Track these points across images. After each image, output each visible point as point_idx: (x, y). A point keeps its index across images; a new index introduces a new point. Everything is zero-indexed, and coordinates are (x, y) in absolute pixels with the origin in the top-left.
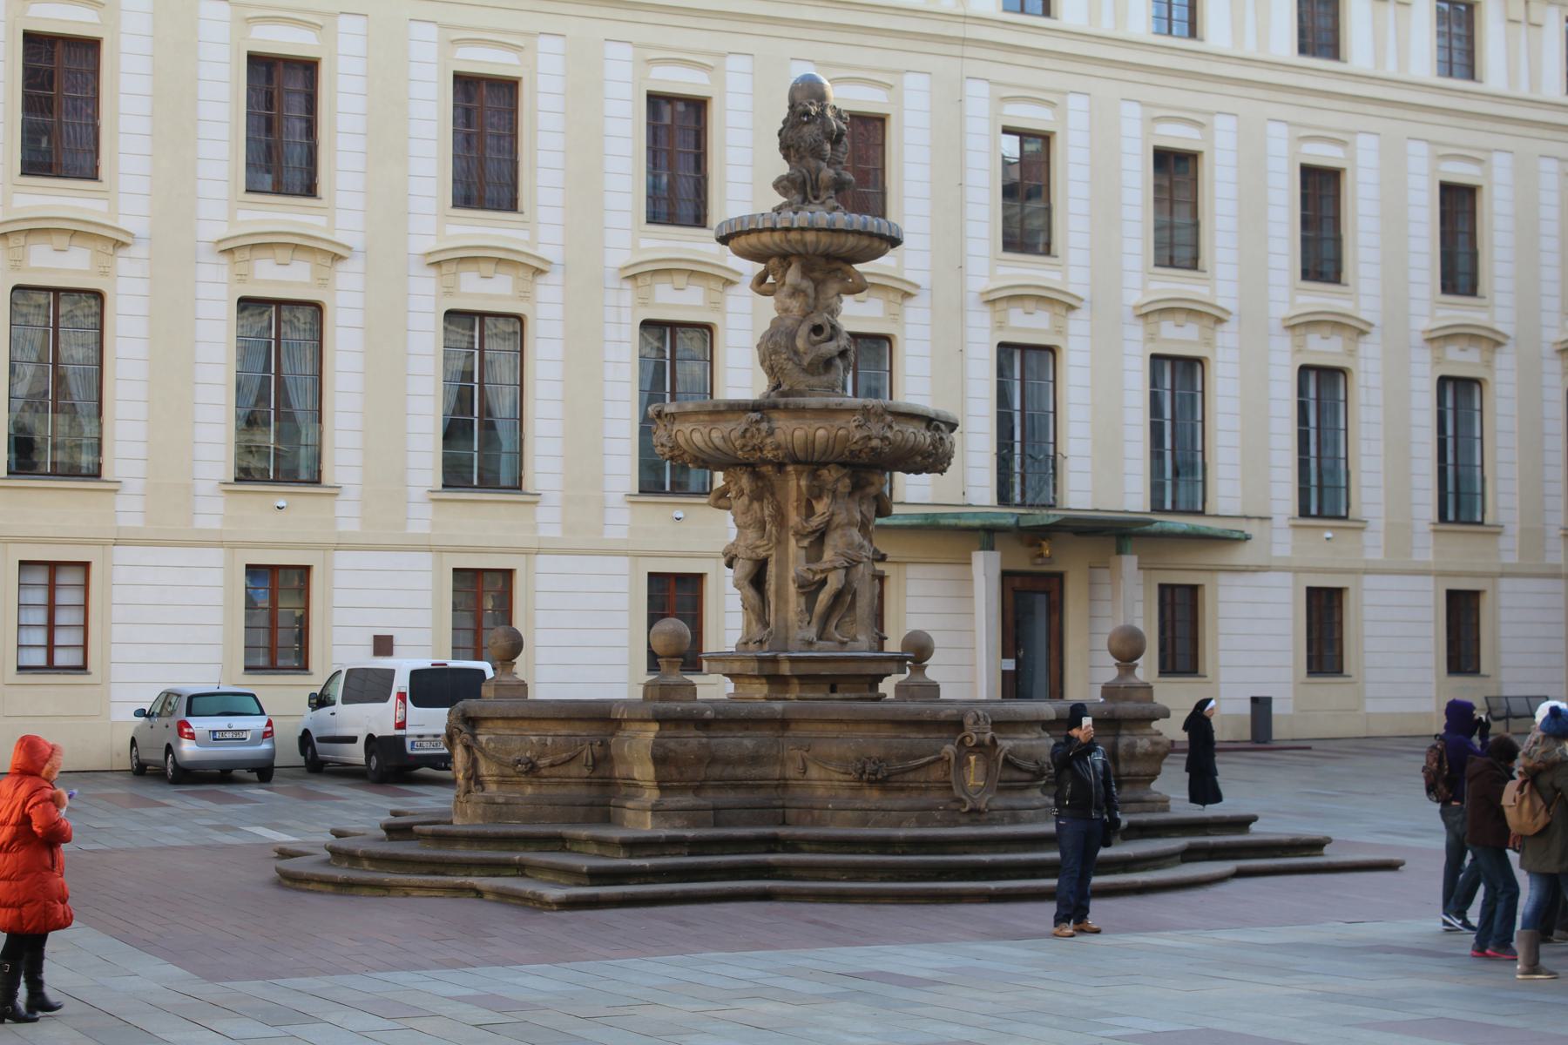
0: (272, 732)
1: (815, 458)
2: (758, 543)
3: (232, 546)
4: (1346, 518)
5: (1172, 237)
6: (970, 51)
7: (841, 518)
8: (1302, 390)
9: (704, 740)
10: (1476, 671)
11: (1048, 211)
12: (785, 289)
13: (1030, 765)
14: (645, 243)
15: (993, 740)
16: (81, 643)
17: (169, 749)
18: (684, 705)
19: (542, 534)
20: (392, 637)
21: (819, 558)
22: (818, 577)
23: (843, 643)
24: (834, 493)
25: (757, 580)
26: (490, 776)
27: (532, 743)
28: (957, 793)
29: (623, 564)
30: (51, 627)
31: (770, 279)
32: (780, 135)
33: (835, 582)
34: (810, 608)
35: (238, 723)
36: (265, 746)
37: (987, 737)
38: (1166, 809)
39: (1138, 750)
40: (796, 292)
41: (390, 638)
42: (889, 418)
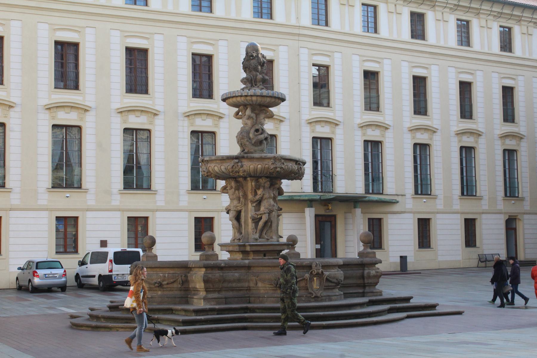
0: (66, 274)
1: (257, 176)
2: (238, 205)
3: (51, 210)
4: (430, 195)
5: (370, 100)
6: (301, 38)
7: (267, 195)
8: (415, 152)
9: (221, 274)
10: (474, 245)
11: (328, 92)
12: (246, 116)
13: (335, 281)
14: (192, 105)
15: (322, 272)
17: (30, 281)
18: (214, 262)
19: (158, 204)
20: (106, 241)
21: (259, 210)
22: (259, 217)
23: (268, 239)
24: (264, 187)
25: (238, 218)
27: (160, 276)
28: (310, 291)
29: (185, 214)
31: (240, 113)
32: (243, 63)
33: (265, 218)
34: (256, 227)
35: (54, 271)
36: (64, 279)
37: (320, 271)
38: (381, 295)
39: (371, 275)
40: (249, 118)
42: (283, 161)
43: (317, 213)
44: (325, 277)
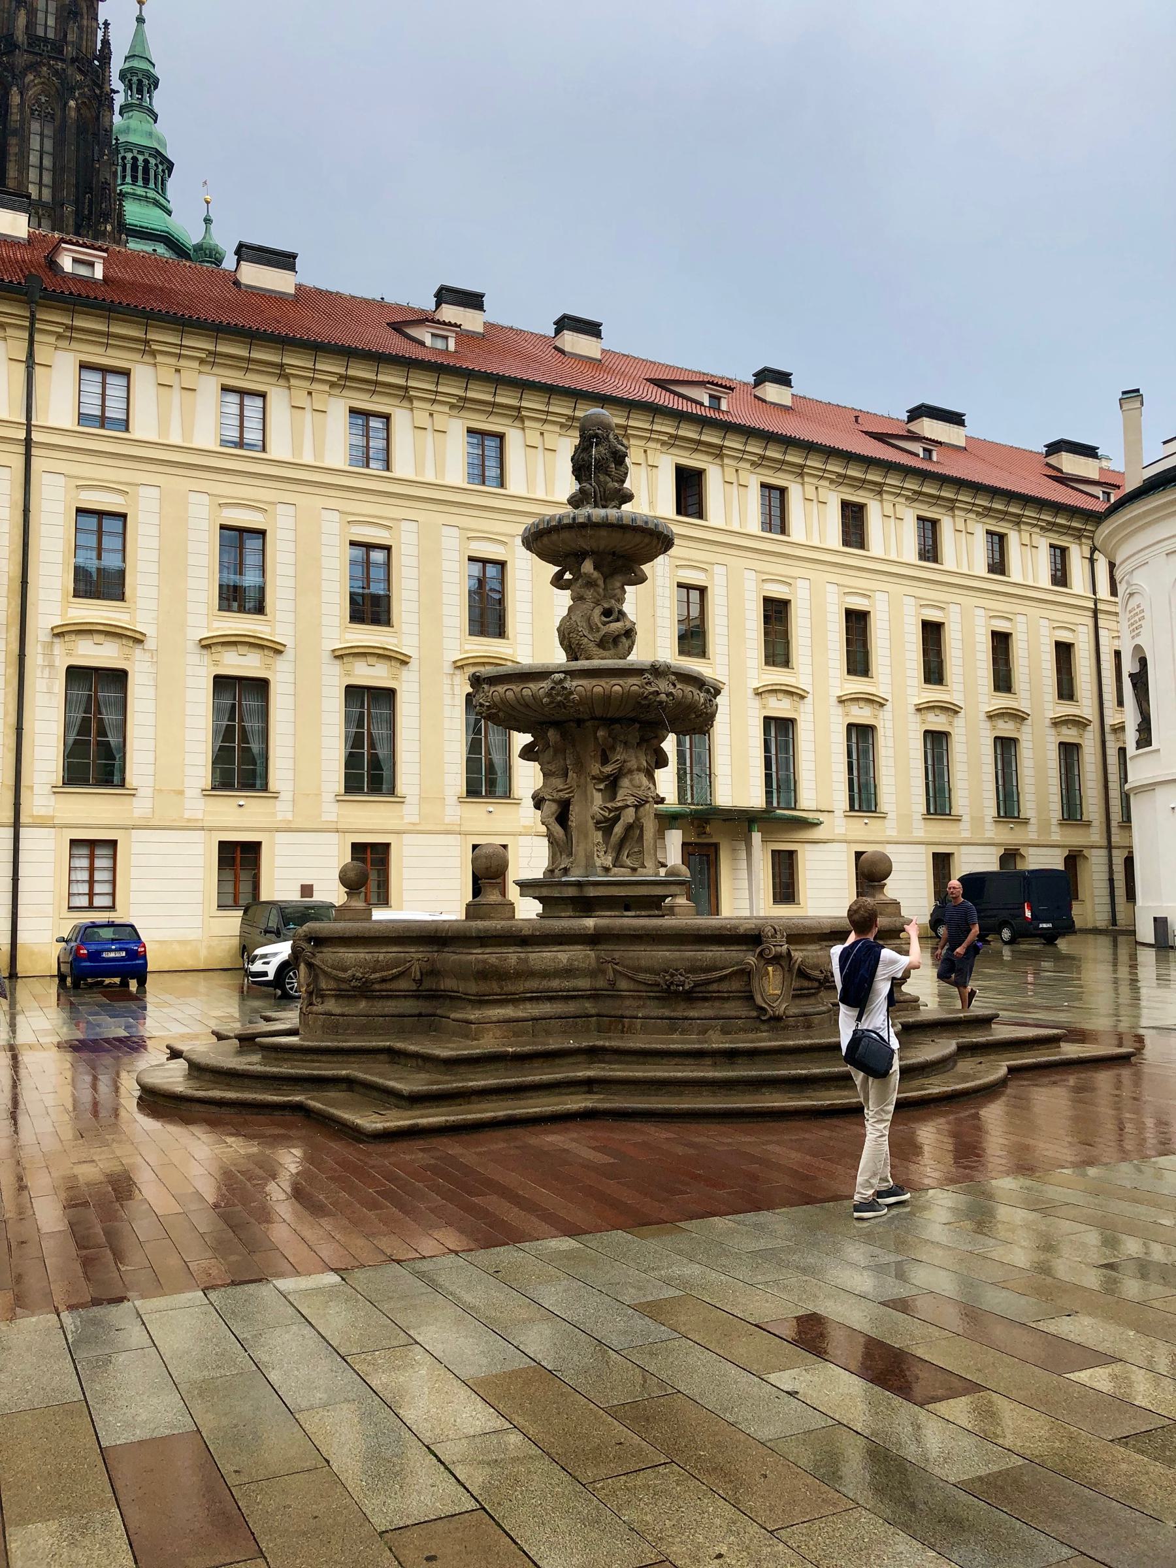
1: (609, 716)
2: (561, 787)
8: (849, 739)
16: (111, 891)
21: (613, 798)
25: (562, 818)
26: (329, 990)
30: (91, 882)
31: (568, 576)
32: (572, 460)
41: (311, 886)
43: (685, 841)
44: (796, 966)
